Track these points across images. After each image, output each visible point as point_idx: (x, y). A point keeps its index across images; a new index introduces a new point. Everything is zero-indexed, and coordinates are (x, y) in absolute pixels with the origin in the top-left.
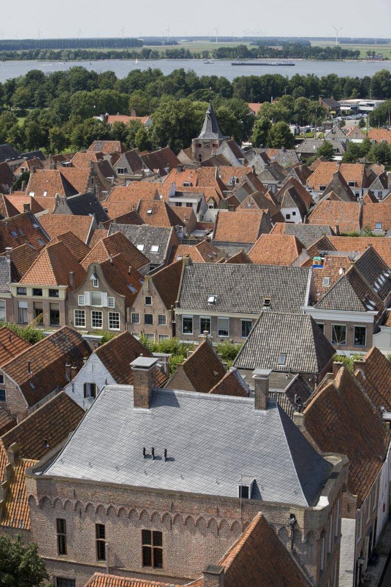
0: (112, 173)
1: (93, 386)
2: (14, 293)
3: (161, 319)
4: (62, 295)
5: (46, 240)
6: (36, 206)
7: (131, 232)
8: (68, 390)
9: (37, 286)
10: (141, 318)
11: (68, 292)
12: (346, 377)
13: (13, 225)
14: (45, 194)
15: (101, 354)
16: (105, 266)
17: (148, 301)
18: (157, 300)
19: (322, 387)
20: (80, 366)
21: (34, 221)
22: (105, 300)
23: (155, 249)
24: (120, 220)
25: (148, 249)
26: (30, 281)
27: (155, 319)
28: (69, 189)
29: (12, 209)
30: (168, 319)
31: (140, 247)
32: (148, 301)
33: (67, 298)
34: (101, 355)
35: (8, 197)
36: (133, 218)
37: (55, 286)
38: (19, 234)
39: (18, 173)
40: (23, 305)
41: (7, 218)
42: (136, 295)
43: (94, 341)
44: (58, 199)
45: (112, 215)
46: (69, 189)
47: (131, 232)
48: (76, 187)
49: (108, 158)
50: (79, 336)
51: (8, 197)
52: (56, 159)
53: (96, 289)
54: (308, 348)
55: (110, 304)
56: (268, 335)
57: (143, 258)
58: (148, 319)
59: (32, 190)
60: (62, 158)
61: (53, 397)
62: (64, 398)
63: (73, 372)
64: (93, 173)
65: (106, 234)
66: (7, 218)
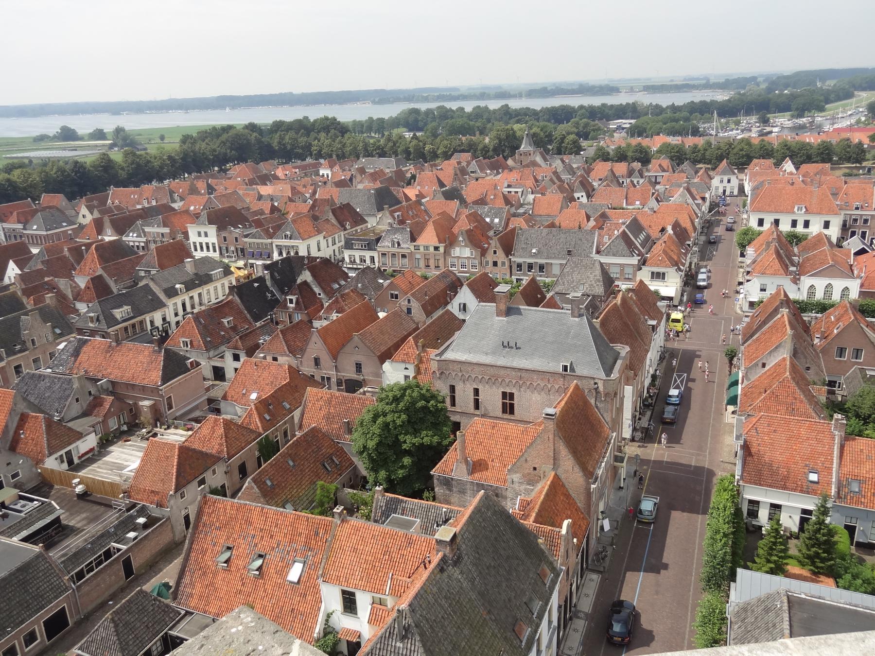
0: (467, 174)
1: (465, 305)
2: (412, 249)
3: (503, 264)
4: (442, 250)
5: (430, 217)
6: (420, 196)
7: (483, 210)
8: (449, 307)
9: (426, 244)
10: (491, 264)
11: (445, 248)
12: (624, 300)
13: (410, 207)
14: (427, 187)
15: (469, 286)
16: (469, 232)
17: (495, 252)
18: (501, 254)
19: (608, 305)
20: (456, 293)
21: (421, 204)
22: (467, 252)
23: (497, 220)
24: (476, 203)
25: (492, 221)
26: (421, 241)
27: (499, 264)
28: (441, 184)
29: (407, 198)
30: (507, 264)
31: (488, 220)
32: (495, 252)
33: (445, 252)
34: (470, 286)
35: (404, 190)
36: (482, 202)
37: (437, 245)
38: (413, 213)
39: (409, 175)
40: (418, 256)
41: (404, 203)
42: (487, 249)
43: (464, 277)
44: (435, 190)
45: (469, 200)
46: (441, 184)
47: (483, 210)
48: (445, 183)
49: (464, 164)
50: (455, 274)
51: (404, 190)
52: (432, 166)
53: (462, 246)
54: (598, 280)
55: (472, 255)
56: (573, 272)
57: (489, 226)
58: (495, 264)
59: (418, 185)
60: (435, 165)
61: (440, 312)
62: (449, 313)
63: (452, 297)
64: (456, 175)
65: (467, 212)
66: (404, 203)
